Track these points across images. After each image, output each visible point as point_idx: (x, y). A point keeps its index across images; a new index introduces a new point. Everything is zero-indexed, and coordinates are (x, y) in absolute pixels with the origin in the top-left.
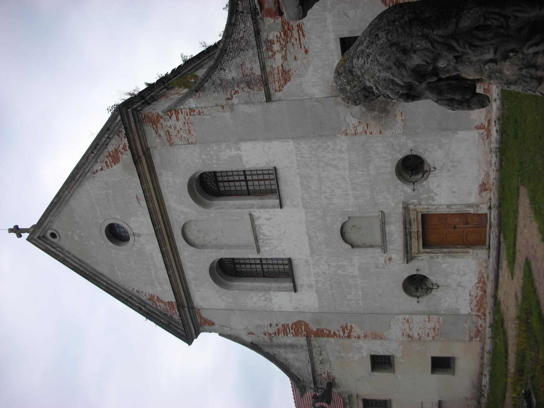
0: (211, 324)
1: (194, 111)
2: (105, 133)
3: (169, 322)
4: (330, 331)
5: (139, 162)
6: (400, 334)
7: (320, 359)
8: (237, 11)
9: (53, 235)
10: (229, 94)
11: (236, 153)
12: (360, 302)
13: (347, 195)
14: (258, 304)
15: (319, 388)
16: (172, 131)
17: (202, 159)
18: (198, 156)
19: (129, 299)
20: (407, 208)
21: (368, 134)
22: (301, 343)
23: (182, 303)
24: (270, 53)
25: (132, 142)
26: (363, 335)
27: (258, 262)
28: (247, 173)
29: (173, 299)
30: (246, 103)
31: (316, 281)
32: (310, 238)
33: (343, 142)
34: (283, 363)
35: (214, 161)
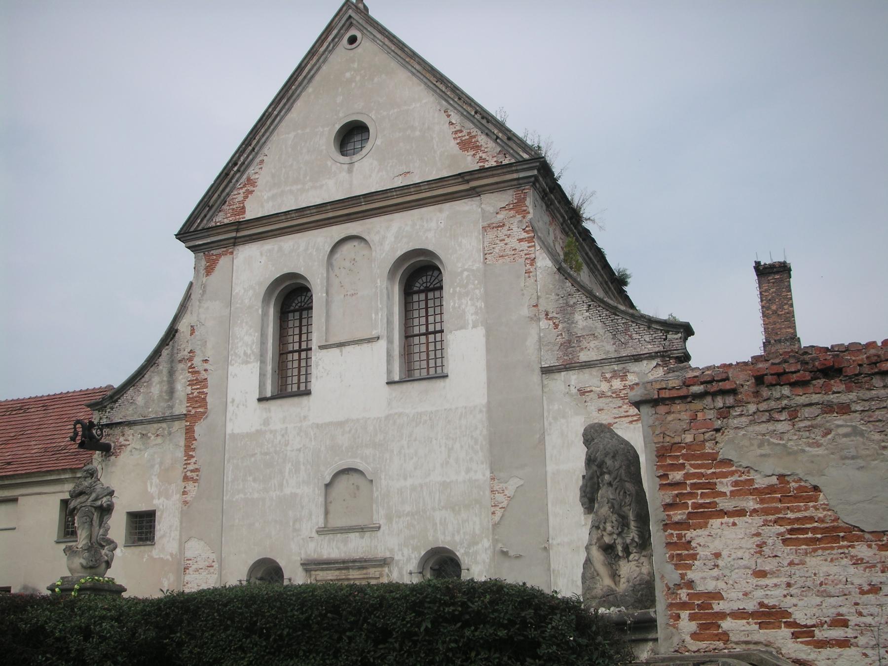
0: (209, 270)
1: (532, 265)
2: (505, 134)
3: (213, 206)
4: (194, 450)
5: (460, 180)
7: (149, 435)
8: (667, 332)
9: (353, 40)
10: (554, 315)
11: (470, 322)
12: (242, 496)
13: (405, 479)
14: (240, 344)
15: (101, 430)
16: (504, 231)
17: (462, 272)
19: (250, 148)
20: (385, 564)
21: (493, 509)
24: (608, 376)
25: (491, 173)
27: (304, 346)
28: (438, 335)
29: (249, 215)
30: (540, 338)
31: (276, 431)
32: (341, 424)
33: (482, 473)
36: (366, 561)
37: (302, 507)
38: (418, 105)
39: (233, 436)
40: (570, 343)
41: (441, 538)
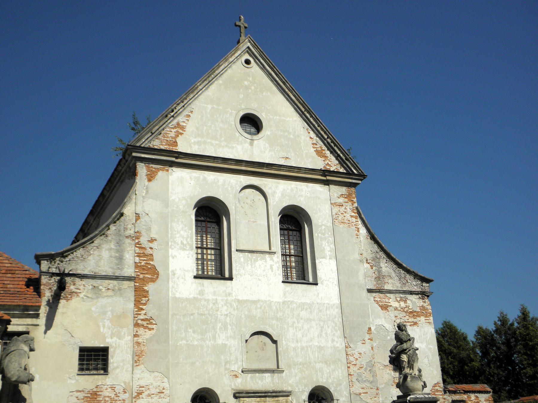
4: (145, 304)
6: (142, 383)
9: (247, 62)
12: (184, 342)
14: (178, 236)
17: (321, 226)
18: (324, 223)
19: (183, 104)
22: (125, 269)
23: (181, 158)
24: (398, 299)
26: (140, 340)
31: (208, 300)
32: (255, 302)
33: (340, 344)
34: (93, 242)
35: (320, 235)
36: (276, 392)
37: (231, 354)
38: (291, 120)
39: (176, 299)
40: (379, 277)
41: (321, 380)
